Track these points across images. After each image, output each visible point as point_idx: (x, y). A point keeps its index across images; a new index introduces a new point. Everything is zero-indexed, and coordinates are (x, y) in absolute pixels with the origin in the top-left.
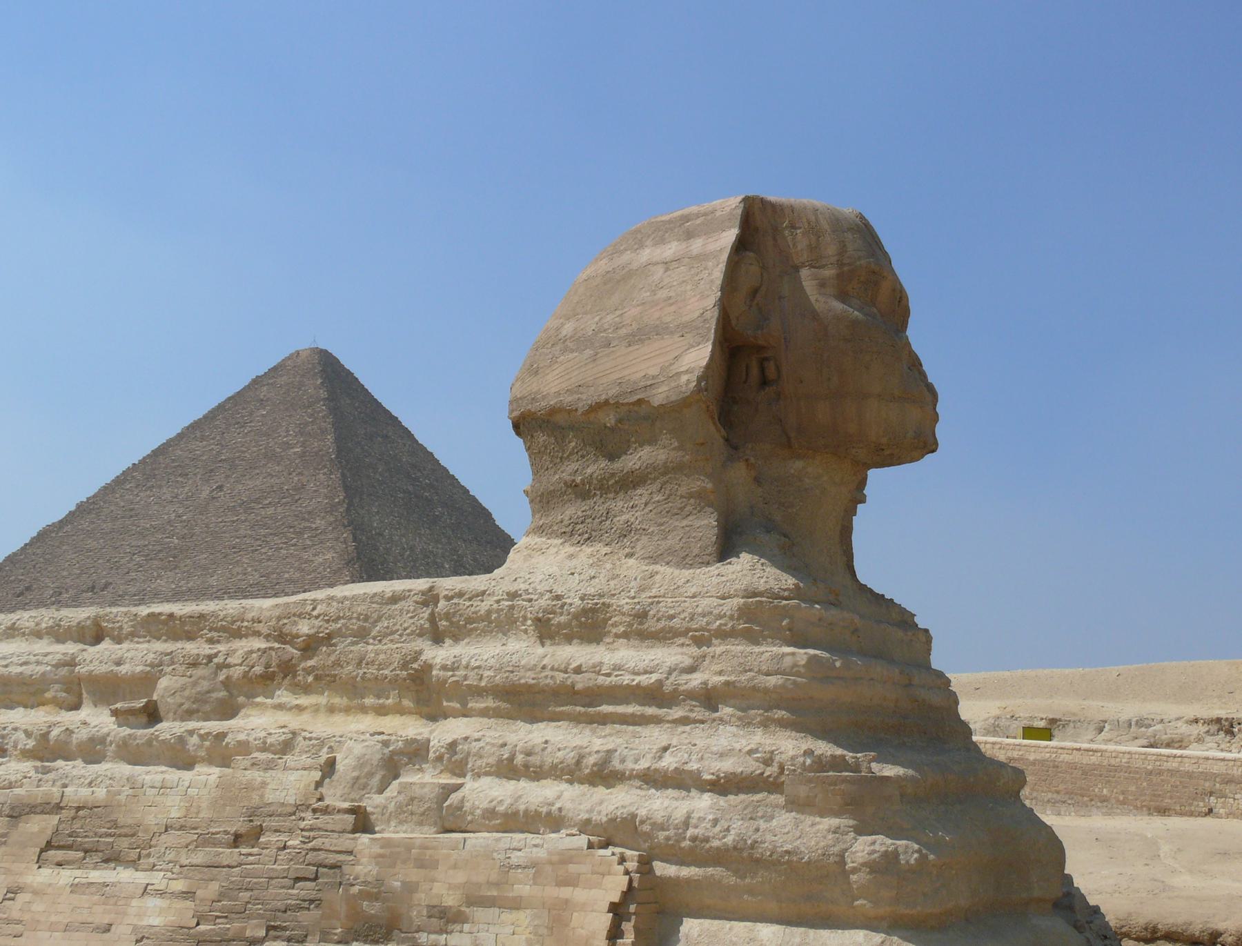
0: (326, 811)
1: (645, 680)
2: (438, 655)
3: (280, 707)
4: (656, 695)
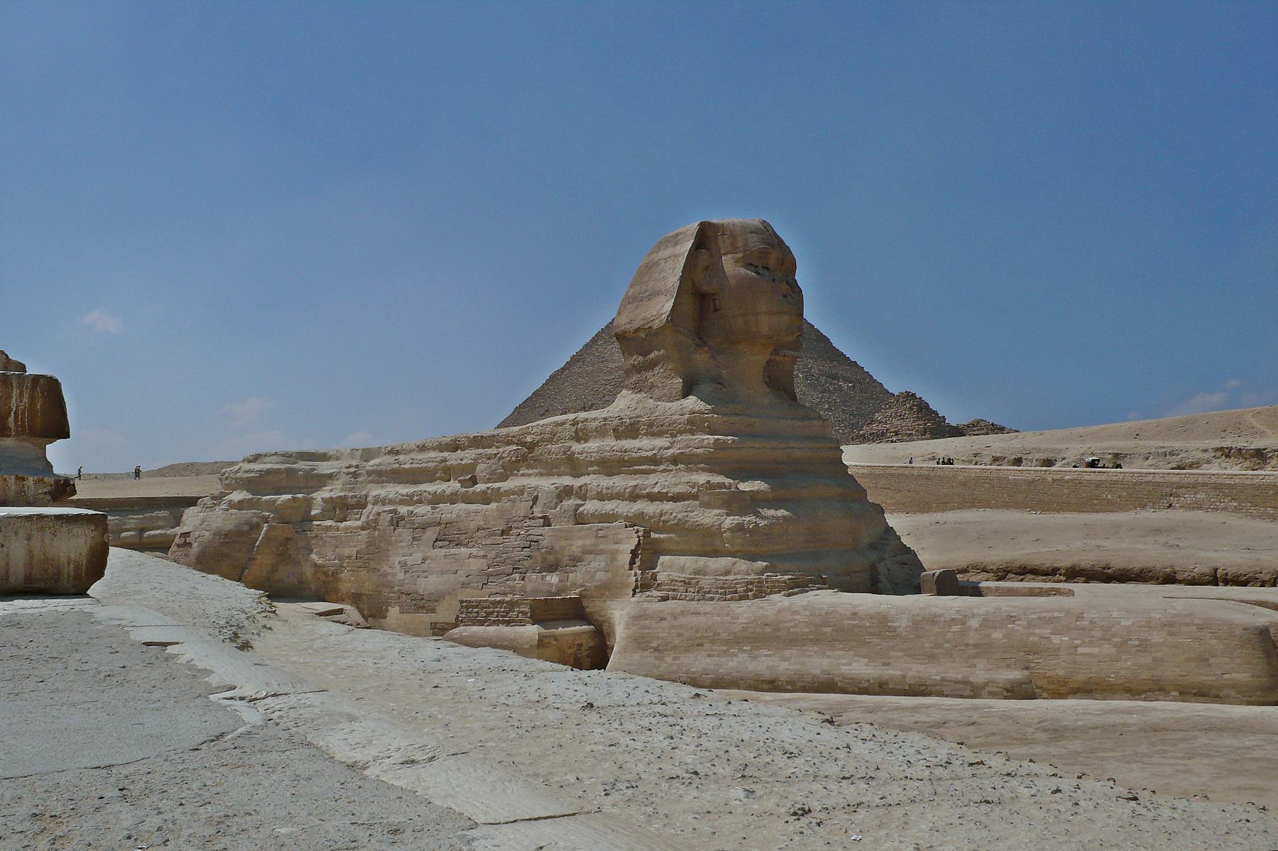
0: (533, 518)
1: (650, 454)
2: (577, 447)
3: (523, 475)
4: (655, 461)
